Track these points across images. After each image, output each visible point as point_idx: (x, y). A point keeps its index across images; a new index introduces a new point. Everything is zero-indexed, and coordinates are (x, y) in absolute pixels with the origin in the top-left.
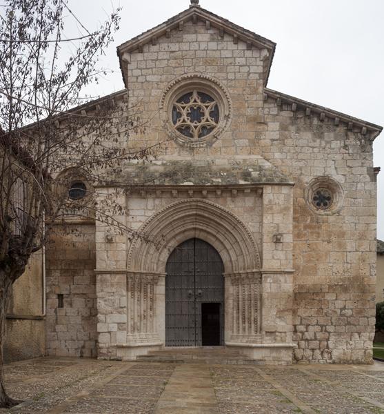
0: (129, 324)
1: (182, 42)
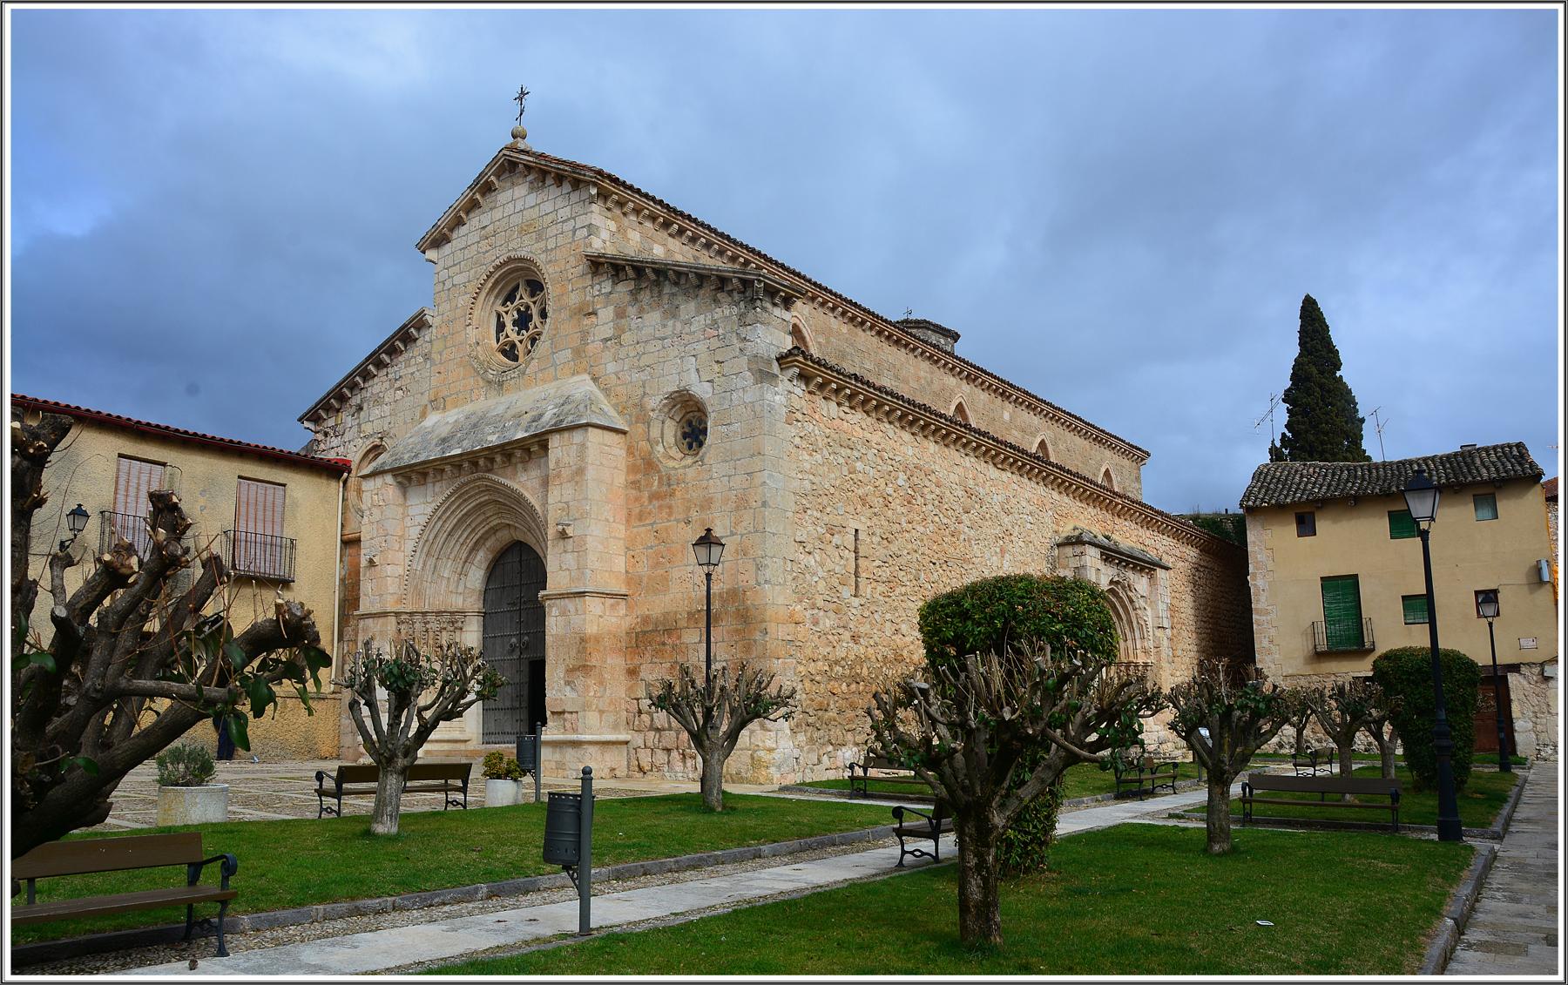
1: (495, 207)
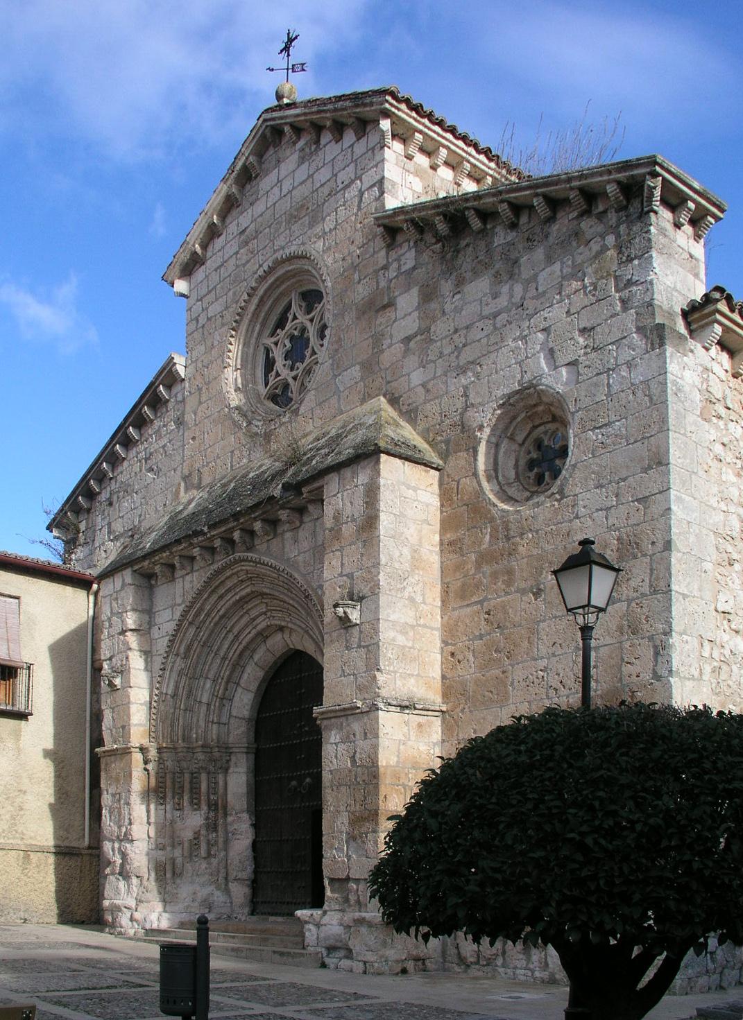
1: (257, 199)
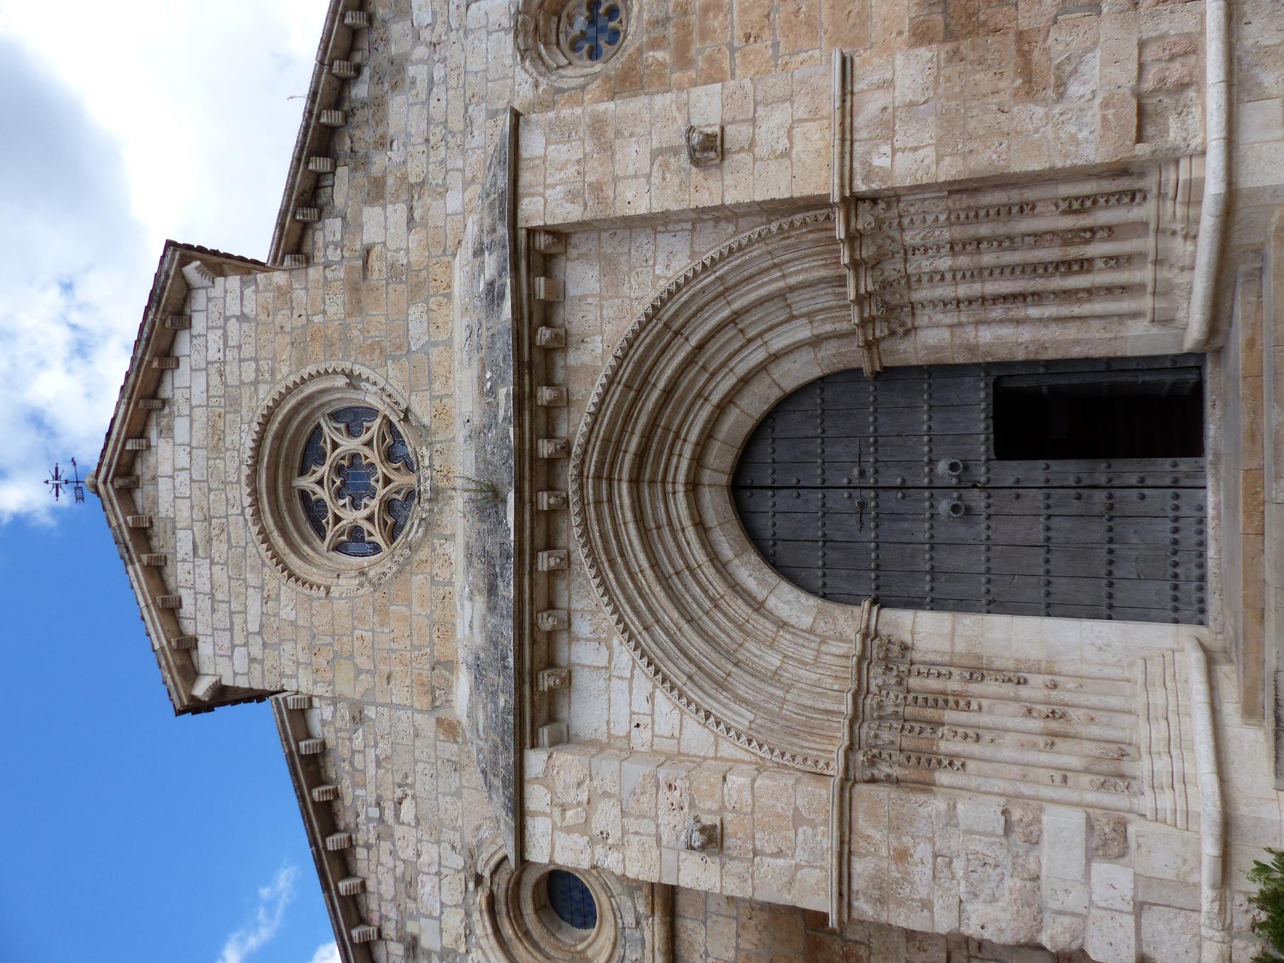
0: (1092, 797)
1: (173, 520)
